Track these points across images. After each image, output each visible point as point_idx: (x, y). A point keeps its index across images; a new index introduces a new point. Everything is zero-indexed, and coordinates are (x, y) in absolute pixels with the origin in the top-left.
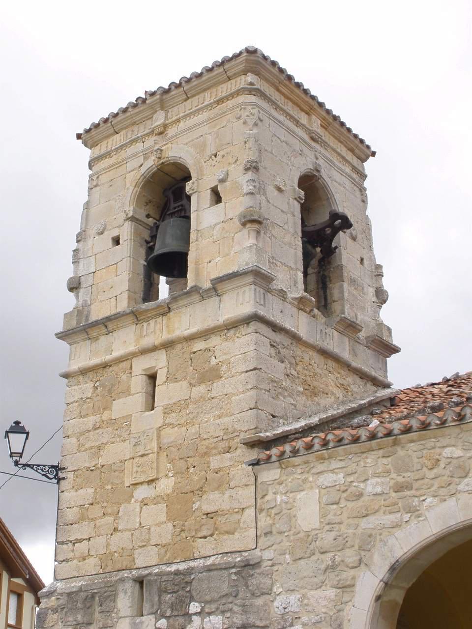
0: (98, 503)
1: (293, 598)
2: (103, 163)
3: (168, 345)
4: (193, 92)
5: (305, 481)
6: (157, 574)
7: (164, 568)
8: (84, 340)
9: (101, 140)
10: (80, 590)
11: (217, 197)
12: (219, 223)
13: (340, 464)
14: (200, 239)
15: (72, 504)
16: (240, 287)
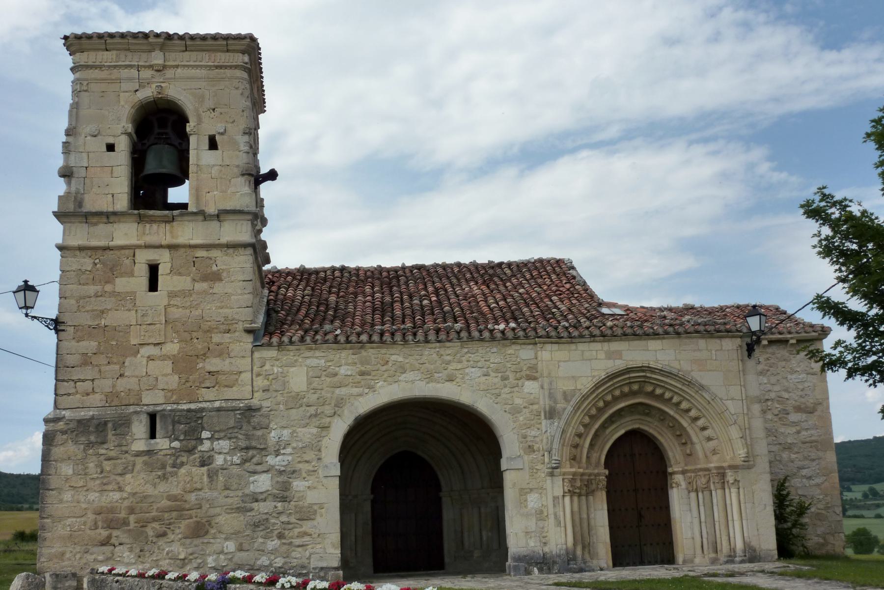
0: (102, 354)
1: (286, 433)
2: (92, 72)
3: (172, 247)
4: (193, 48)
5: (296, 361)
6: (170, 411)
7: (175, 406)
8: (80, 222)
9: (88, 50)
10: (93, 418)
11: (213, 145)
12: (218, 165)
13: (323, 354)
14: (199, 172)
15: (73, 351)
16: (239, 220)
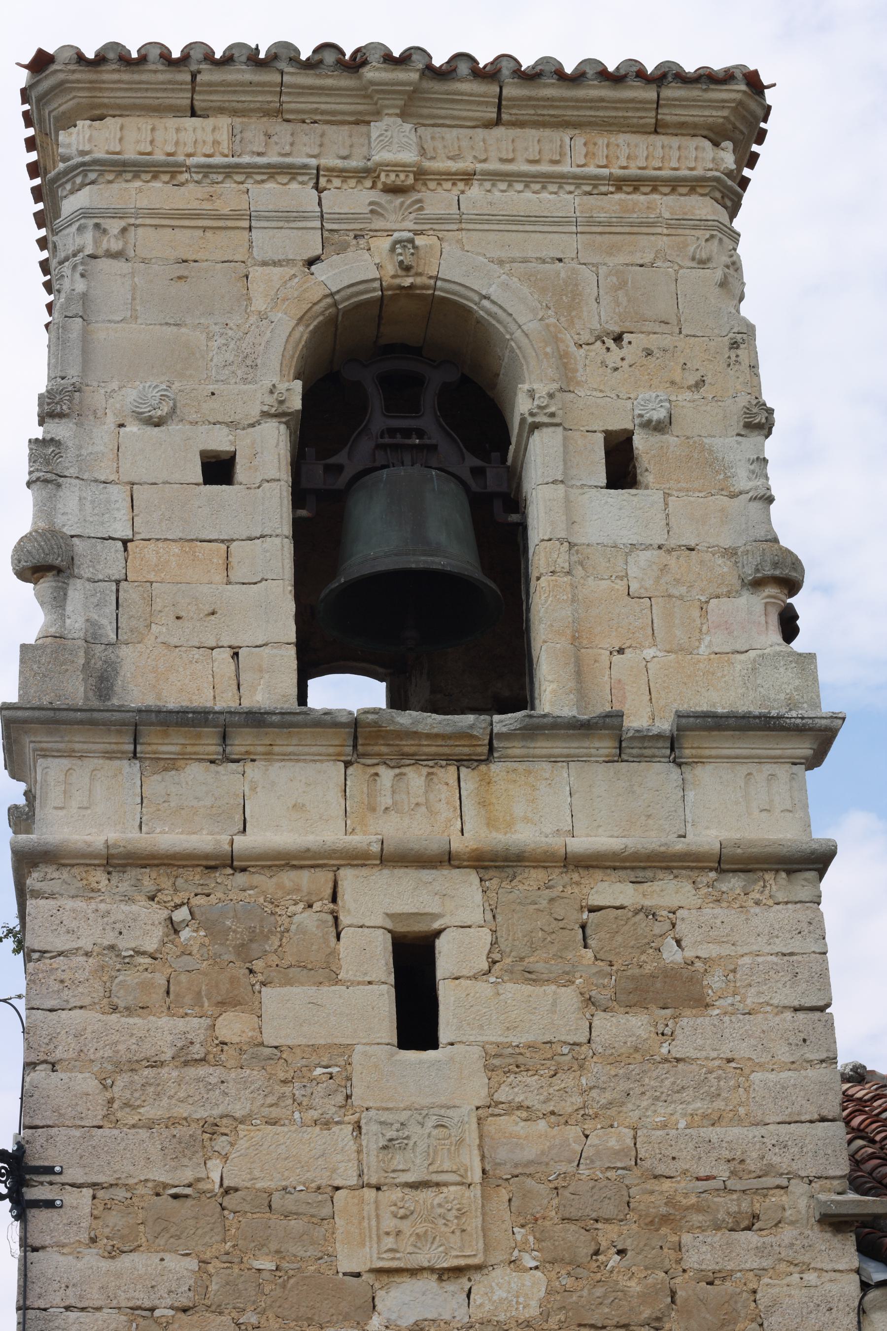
2: (140, 190)
4: (526, 113)
8: (110, 756)
9: (123, 110)
12: (648, 547)
14: (579, 571)
15: (95, 1298)
16: (760, 760)
